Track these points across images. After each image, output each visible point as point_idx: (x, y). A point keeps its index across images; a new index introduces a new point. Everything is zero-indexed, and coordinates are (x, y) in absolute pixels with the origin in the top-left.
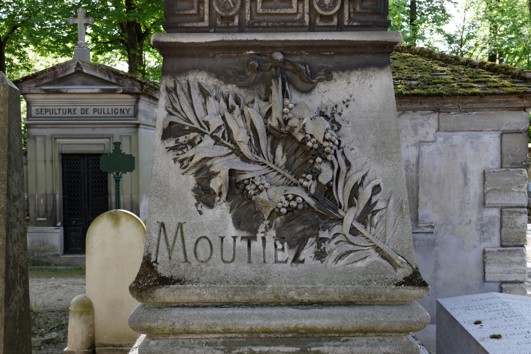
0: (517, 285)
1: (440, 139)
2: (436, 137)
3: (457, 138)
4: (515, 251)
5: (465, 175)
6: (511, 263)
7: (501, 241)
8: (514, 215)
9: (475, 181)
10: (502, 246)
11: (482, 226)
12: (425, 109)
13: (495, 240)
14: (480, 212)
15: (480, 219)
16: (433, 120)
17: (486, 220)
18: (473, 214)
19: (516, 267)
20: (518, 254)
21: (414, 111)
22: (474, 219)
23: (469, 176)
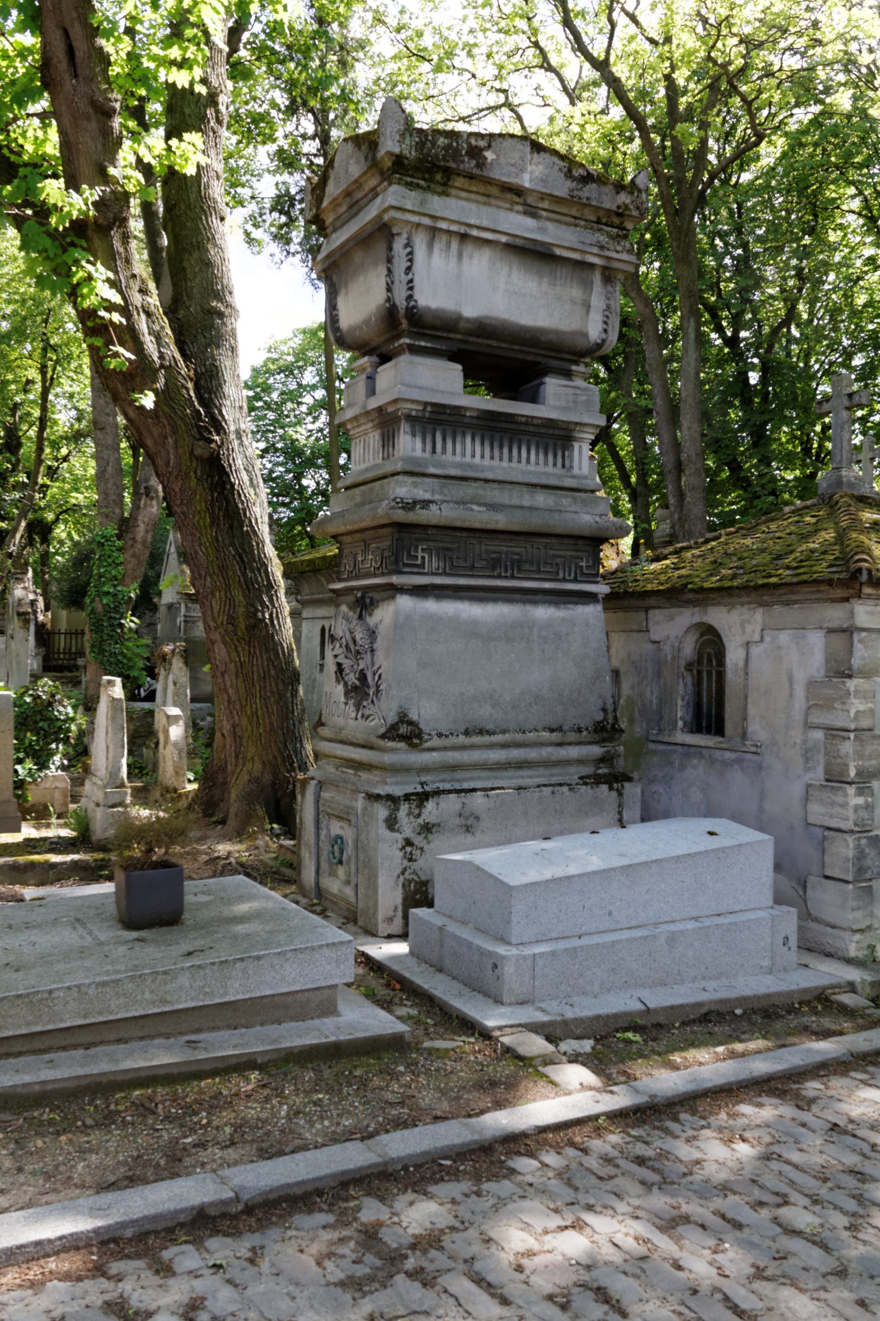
0: (839, 834)
1: (767, 639)
2: (762, 637)
3: (784, 637)
4: (839, 788)
5: (791, 685)
6: (833, 804)
7: (827, 772)
8: (837, 741)
9: (800, 691)
10: (827, 780)
11: (807, 751)
12: (750, 603)
13: (819, 773)
14: (805, 733)
15: (805, 742)
16: (759, 616)
17: (810, 744)
18: (797, 735)
19: (838, 809)
20: (840, 793)
21: (742, 605)
22: (798, 741)
23: (795, 686)
